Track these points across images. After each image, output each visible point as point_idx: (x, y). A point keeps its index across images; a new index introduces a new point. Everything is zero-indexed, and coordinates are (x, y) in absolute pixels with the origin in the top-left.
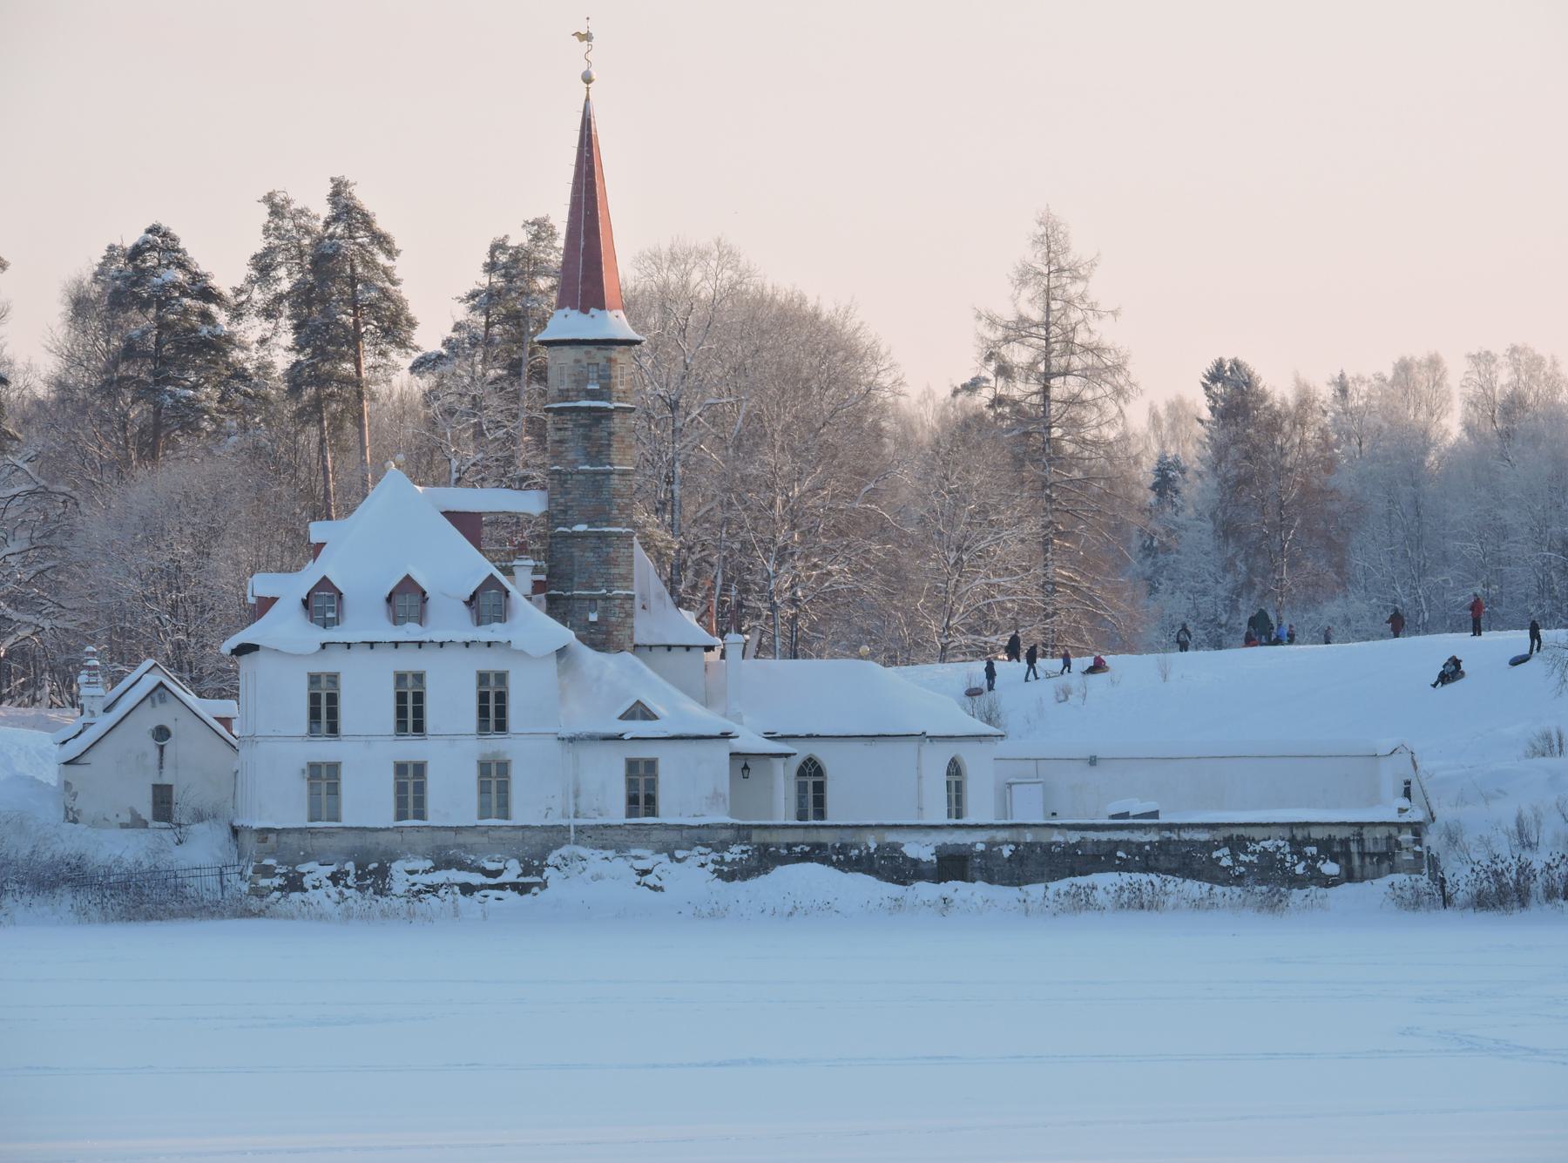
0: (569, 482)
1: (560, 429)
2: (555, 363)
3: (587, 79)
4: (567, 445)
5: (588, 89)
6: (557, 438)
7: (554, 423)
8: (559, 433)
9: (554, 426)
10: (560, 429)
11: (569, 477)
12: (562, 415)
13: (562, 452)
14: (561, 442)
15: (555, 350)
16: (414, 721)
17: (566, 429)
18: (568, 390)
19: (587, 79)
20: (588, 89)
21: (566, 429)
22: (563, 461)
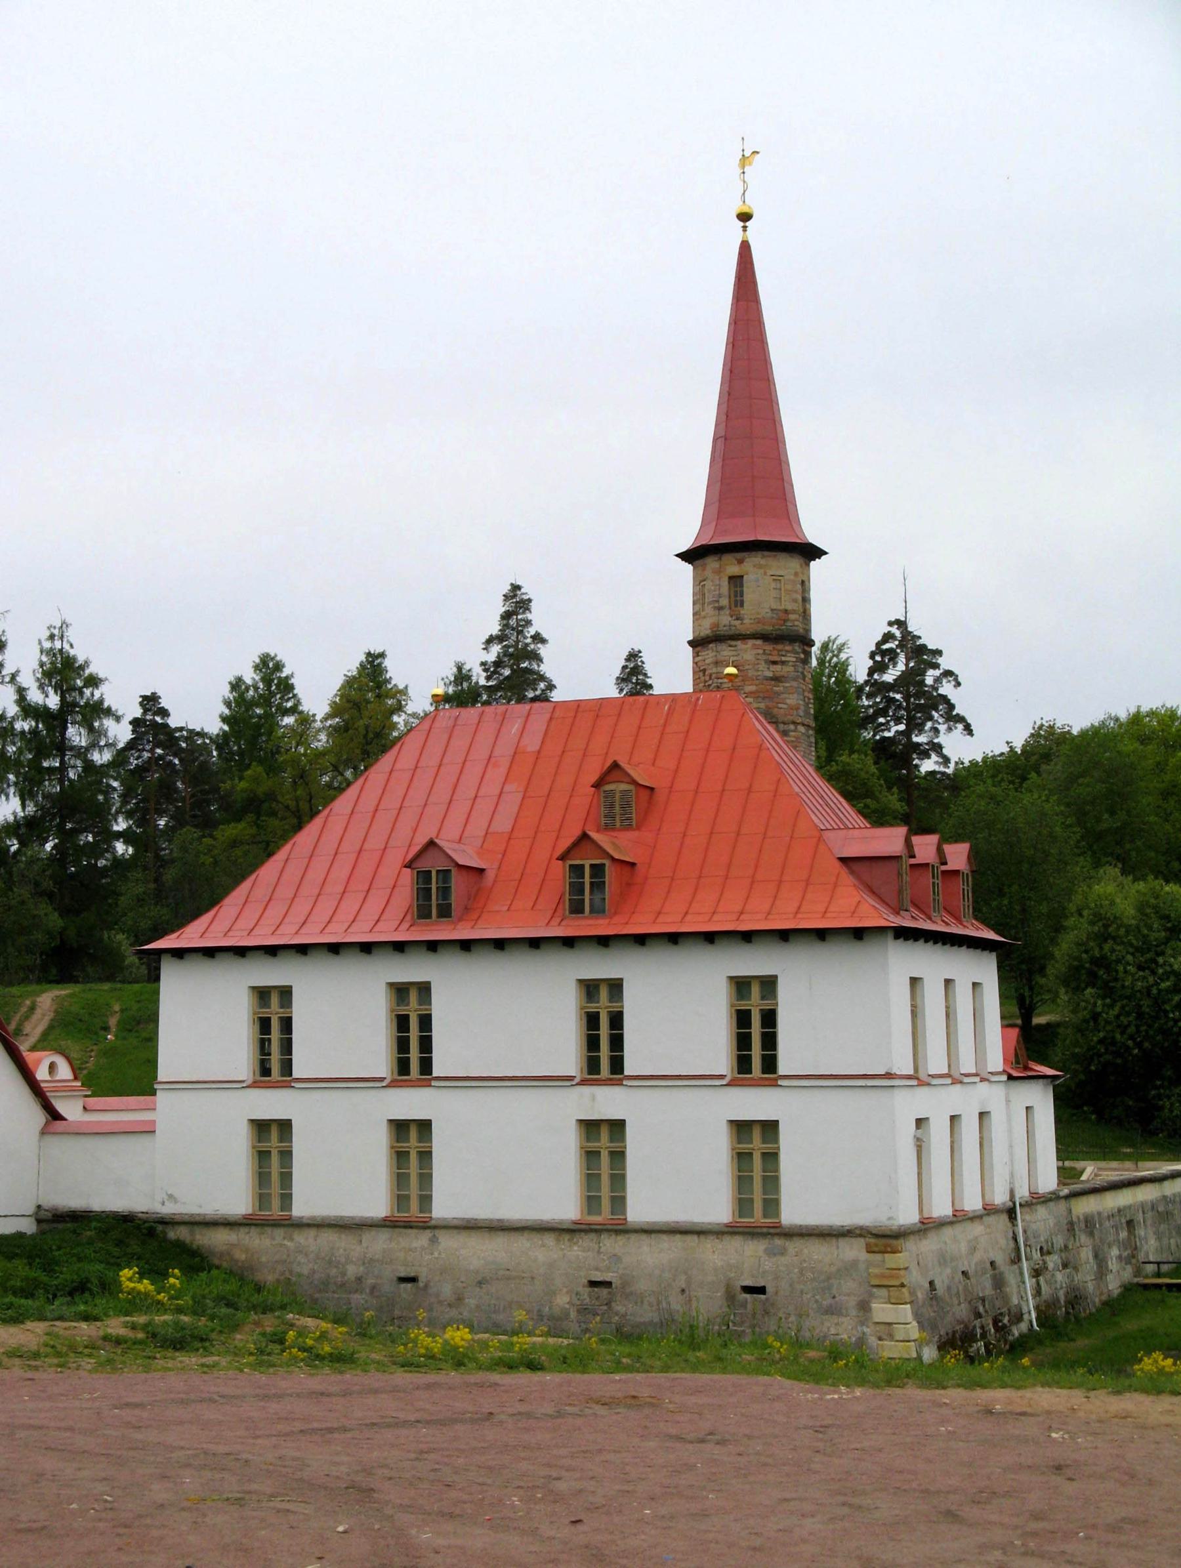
0: (792, 734)
1: (774, 663)
2: (765, 573)
3: (745, 217)
4: (787, 685)
5: (745, 228)
6: (770, 674)
7: (764, 653)
8: (773, 668)
9: (765, 657)
10: (774, 663)
11: (792, 727)
12: (776, 643)
13: (778, 694)
14: (776, 679)
15: (763, 557)
16: (750, 1050)
17: (783, 663)
18: (786, 611)
19: (745, 217)
20: (745, 228)
21: (783, 663)
22: (780, 705)
